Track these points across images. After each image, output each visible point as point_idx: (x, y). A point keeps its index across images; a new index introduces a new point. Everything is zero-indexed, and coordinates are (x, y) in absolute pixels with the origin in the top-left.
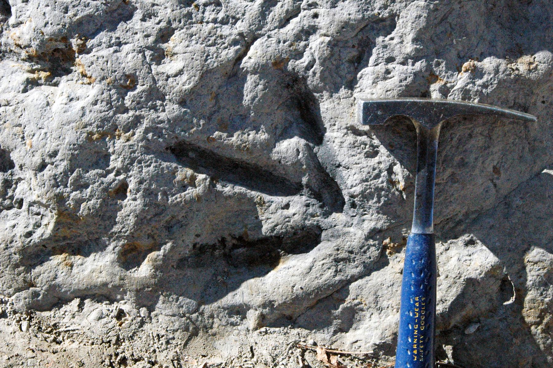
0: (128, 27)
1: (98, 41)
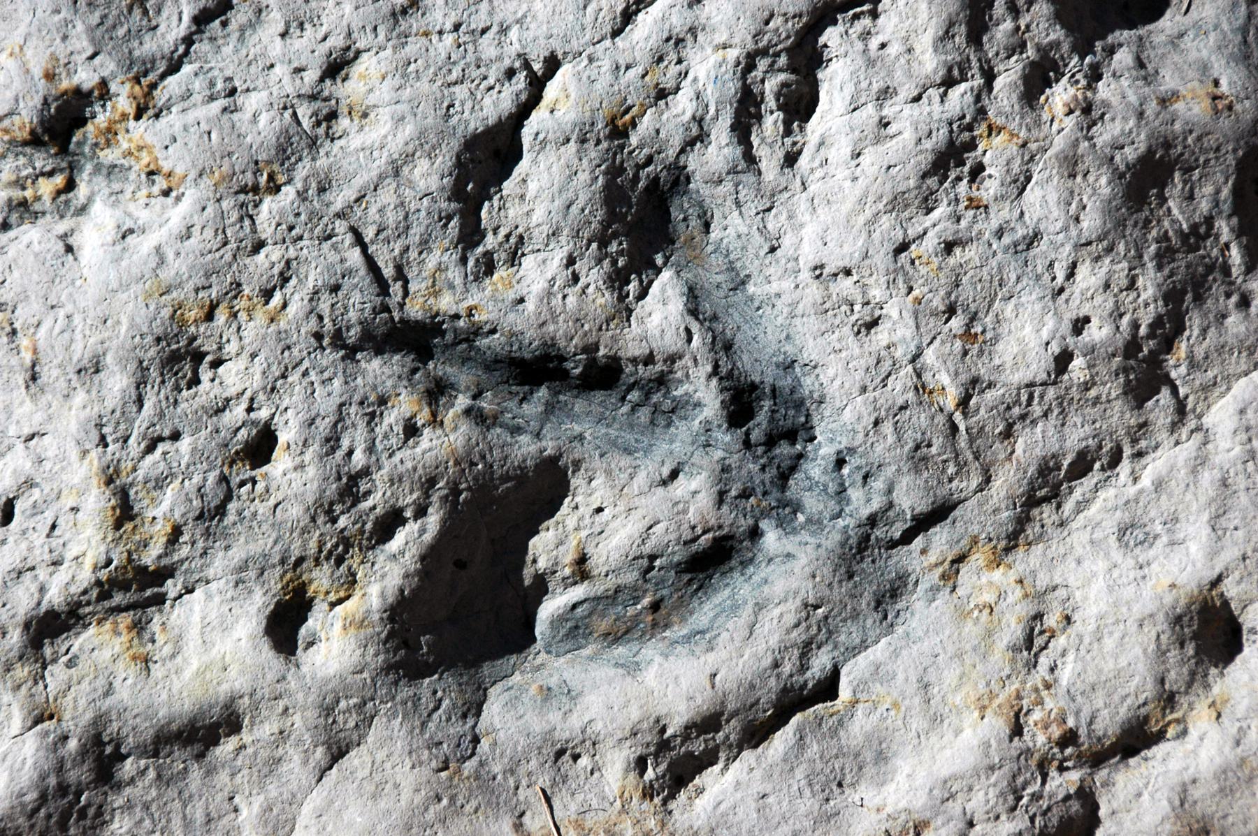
1: (184, 88)
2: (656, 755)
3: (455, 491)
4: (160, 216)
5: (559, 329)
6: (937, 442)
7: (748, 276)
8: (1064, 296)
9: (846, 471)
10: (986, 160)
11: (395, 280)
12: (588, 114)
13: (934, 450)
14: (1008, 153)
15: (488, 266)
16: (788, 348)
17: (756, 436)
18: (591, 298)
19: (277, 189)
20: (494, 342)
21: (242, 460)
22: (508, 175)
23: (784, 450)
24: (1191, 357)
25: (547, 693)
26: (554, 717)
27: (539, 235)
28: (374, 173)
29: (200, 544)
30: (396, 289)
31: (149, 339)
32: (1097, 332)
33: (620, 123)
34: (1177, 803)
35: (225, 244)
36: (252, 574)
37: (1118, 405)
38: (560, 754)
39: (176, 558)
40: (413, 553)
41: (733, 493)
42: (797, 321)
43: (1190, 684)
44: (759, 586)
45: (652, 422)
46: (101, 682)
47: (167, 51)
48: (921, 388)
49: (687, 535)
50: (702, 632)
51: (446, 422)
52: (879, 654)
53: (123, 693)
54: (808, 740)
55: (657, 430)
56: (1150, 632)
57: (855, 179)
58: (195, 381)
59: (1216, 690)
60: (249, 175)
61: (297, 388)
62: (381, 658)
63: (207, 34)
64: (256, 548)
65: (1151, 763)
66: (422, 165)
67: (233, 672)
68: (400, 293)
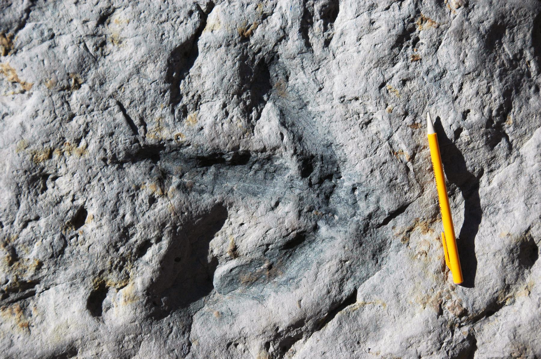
0: (61, 14)
1: (28, 37)
2: (274, 340)
3: (175, 227)
4: (21, 105)
5: (220, 141)
6: (400, 177)
7: (308, 102)
8: (458, 100)
9: (357, 193)
10: (420, 36)
11: (140, 126)
12: (230, 32)
13: (398, 181)
14: (431, 31)
15: (185, 112)
16: (329, 137)
17: (314, 180)
18: (235, 123)
19: (79, 86)
20: (190, 150)
21: (71, 226)
22: (191, 65)
23: (327, 184)
24: (515, 122)
25: (221, 315)
26: (226, 328)
27: (208, 95)
28: (127, 73)
29: (52, 269)
30: (141, 130)
31: (21, 172)
32: (474, 117)
33: (245, 34)
34: (512, 337)
35: (55, 118)
36: (79, 280)
37: (482, 150)
38: (229, 345)
39: (40, 276)
40: (156, 259)
41: (305, 210)
42: (333, 124)
43: (516, 280)
44: (319, 253)
45: (265, 178)
46: (7, 340)
47: (17, 18)
48: (392, 153)
49: (284, 233)
50: (293, 278)
51: (169, 194)
52: (375, 281)
53: (18, 345)
54: (343, 324)
55: (268, 182)
56: (499, 258)
57: (359, 52)
58: (45, 189)
59: (528, 280)
60: (65, 81)
61: (96, 188)
62: (144, 313)
63: (37, 6)
64: (80, 268)
65: (499, 318)
66: (151, 67)
67: (72, 328)
68: (143, 132)
